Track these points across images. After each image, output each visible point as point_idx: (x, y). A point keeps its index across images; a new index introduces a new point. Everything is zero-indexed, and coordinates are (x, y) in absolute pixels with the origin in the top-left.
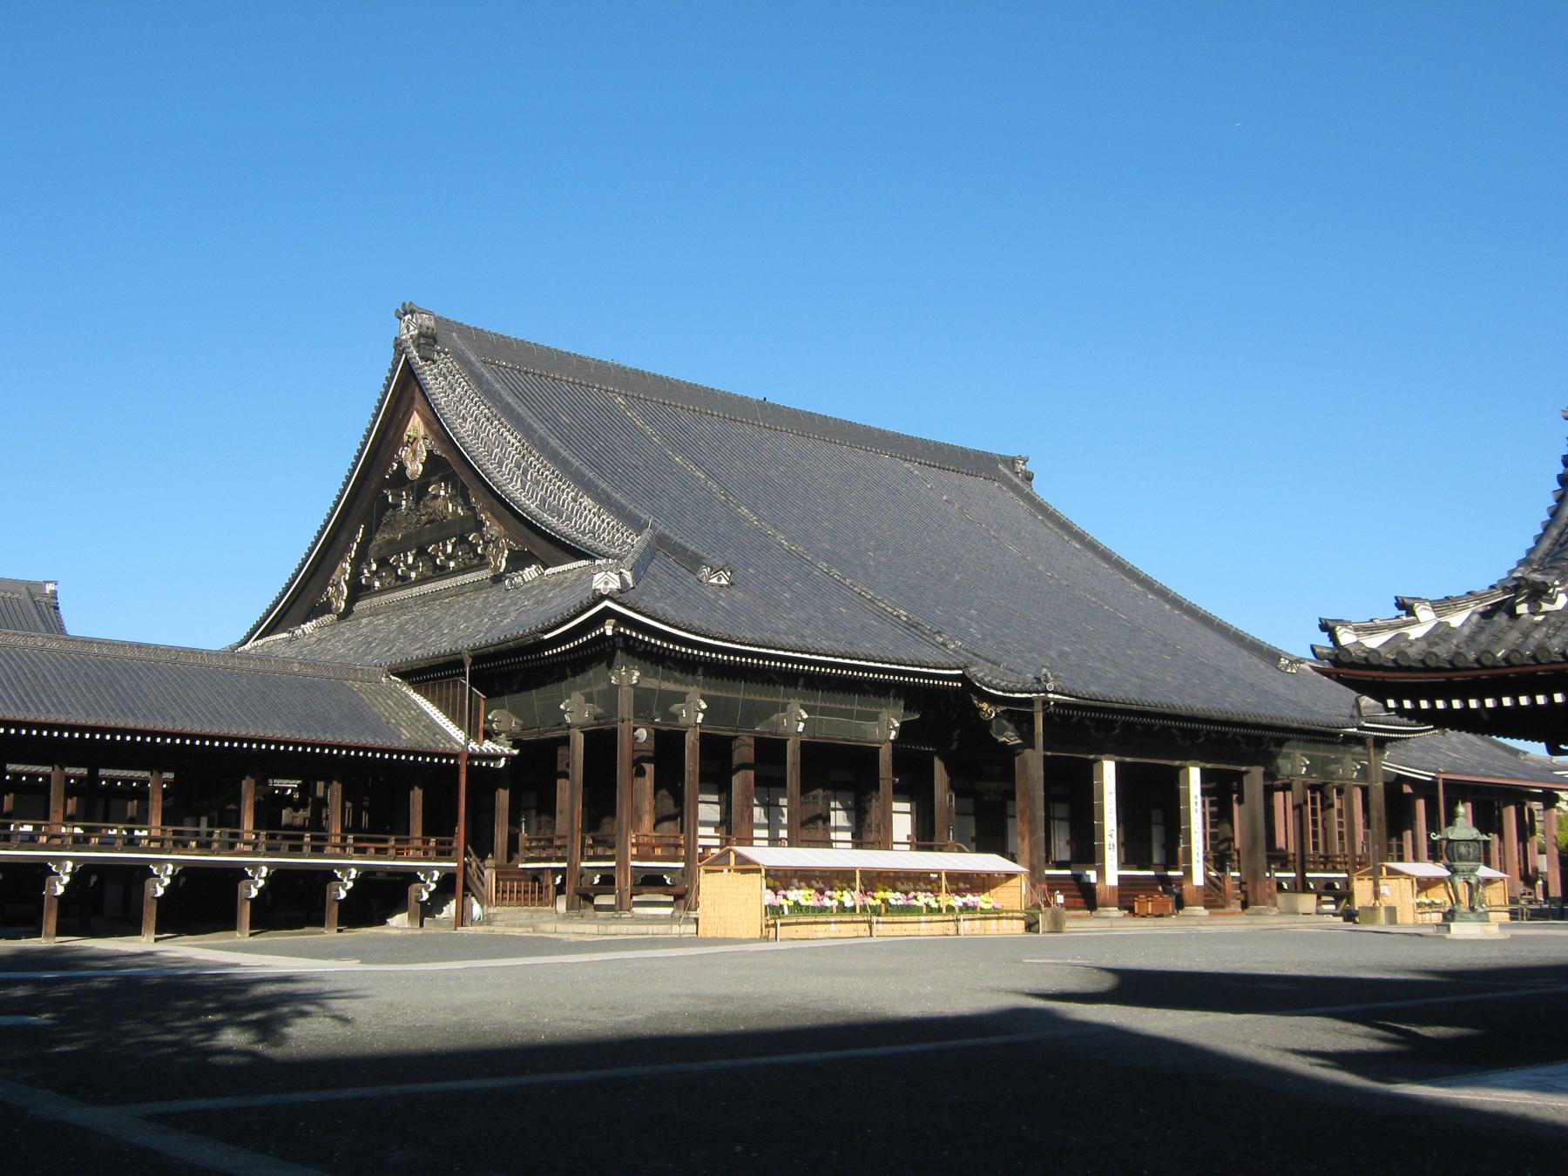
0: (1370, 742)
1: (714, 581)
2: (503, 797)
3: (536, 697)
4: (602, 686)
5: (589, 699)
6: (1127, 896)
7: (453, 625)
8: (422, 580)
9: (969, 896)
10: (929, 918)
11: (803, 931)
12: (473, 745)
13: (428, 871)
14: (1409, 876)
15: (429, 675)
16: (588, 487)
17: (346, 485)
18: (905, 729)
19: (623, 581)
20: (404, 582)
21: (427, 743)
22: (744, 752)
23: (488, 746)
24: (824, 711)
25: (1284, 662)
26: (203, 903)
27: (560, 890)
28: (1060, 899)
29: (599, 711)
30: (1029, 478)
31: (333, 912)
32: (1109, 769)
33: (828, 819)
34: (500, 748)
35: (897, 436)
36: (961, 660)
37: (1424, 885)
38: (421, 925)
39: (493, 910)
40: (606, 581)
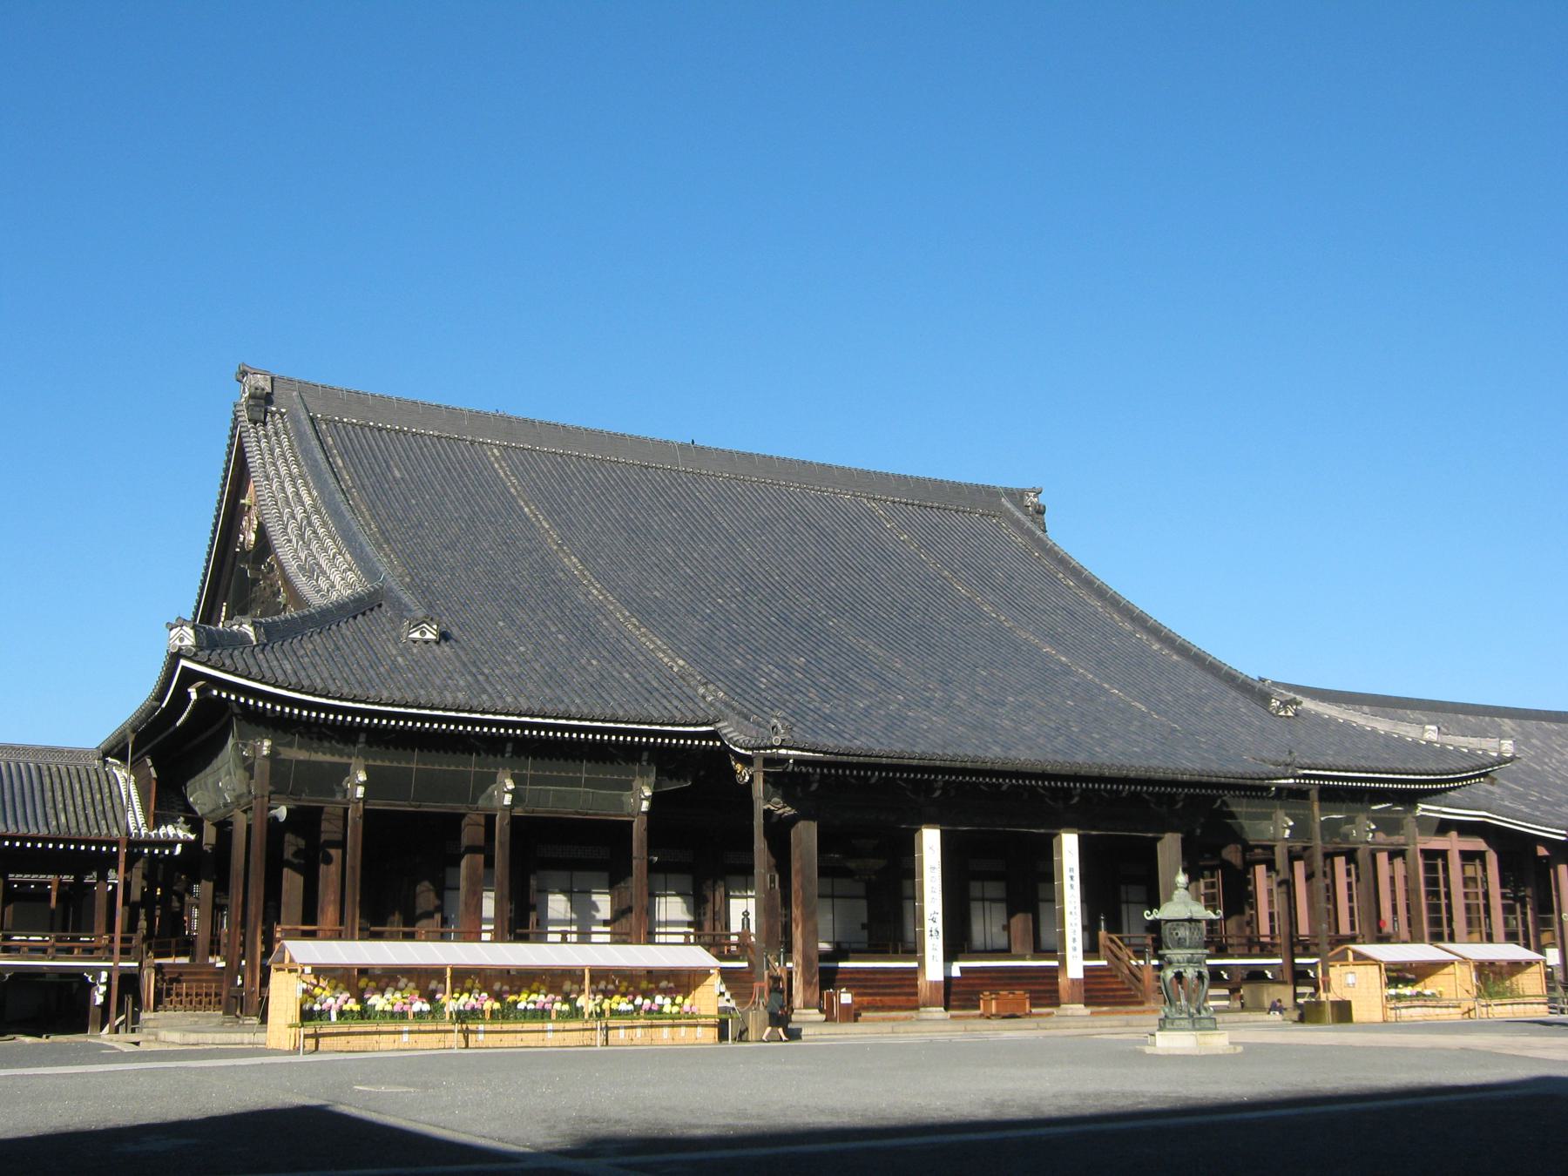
0: (1314, 794)
1: (417, 635)
6: (956, 995)
9: (659, 999)
10: (560, 1026)
11: (357, 1042)
13: (96, 972)
14: (1377, 963)
16: (349, 540)
17: (208, 561)
18: (655, 799)
22: (471, 833)
23: (168, 831)
24: (536, 780)
25: (1275, 703)
28: (846, 998)
30: (1040, 511)
32: (930, 841)
33: (650, 911)
35: (867, 474)
36: (712, 713)
37: (1398, 975)
38: (291, 1026)
39: (152, 1015)
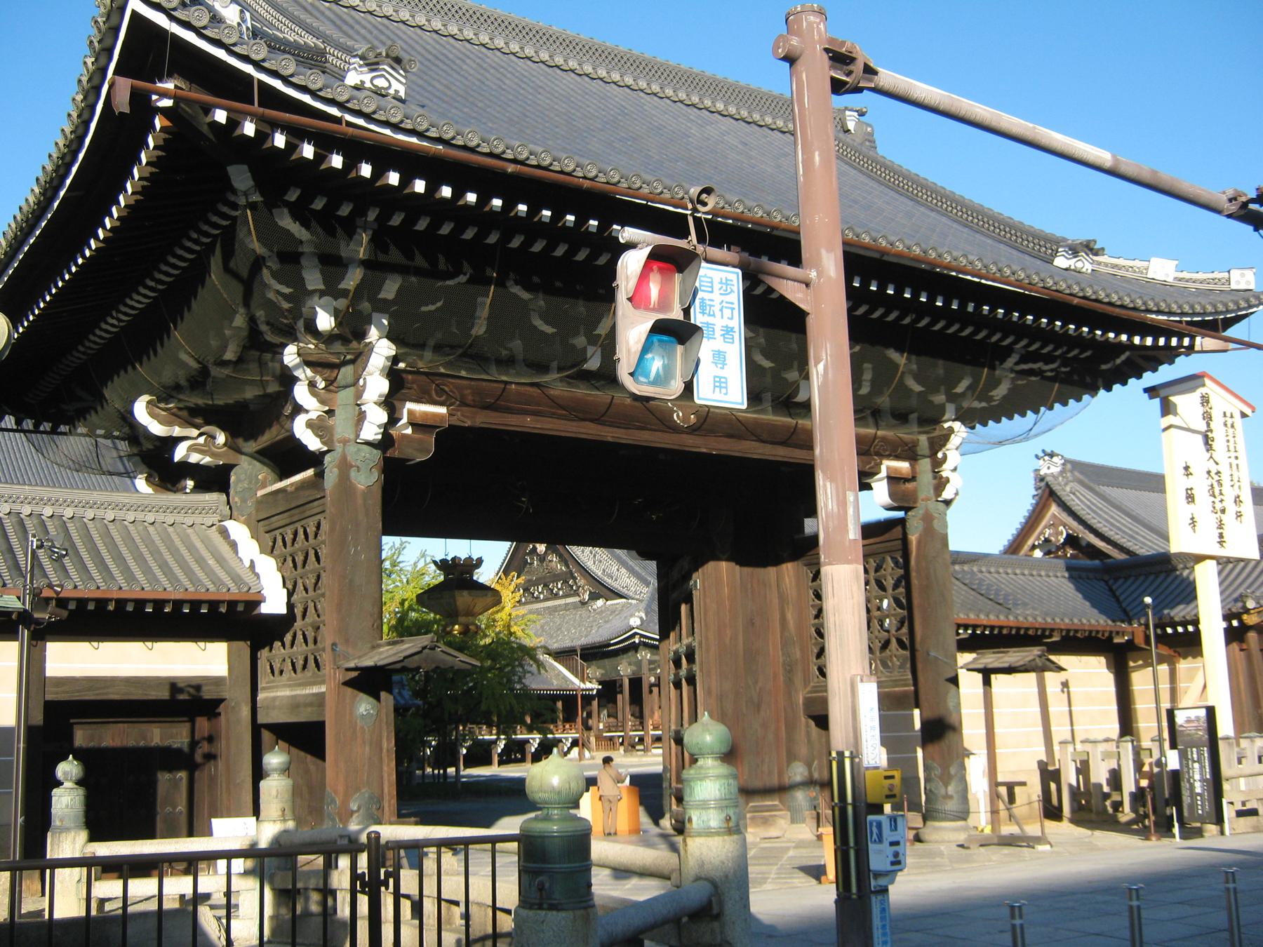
2: (595, 703)
3: (607, 662)
4: (633, 659)
5: (630, 664)
7: (569, 631)
8: (546, 599)
12: (582, 686)
15: (563, 655)
19: (641, 618)
20: (537, 600)
21: (564, 687)
23: (589, 685)
26: (481, 755)
27: (622, 744)
29: (634, 668)
31: (529, 757)
34: (594, 686)
40: (635, 622)
